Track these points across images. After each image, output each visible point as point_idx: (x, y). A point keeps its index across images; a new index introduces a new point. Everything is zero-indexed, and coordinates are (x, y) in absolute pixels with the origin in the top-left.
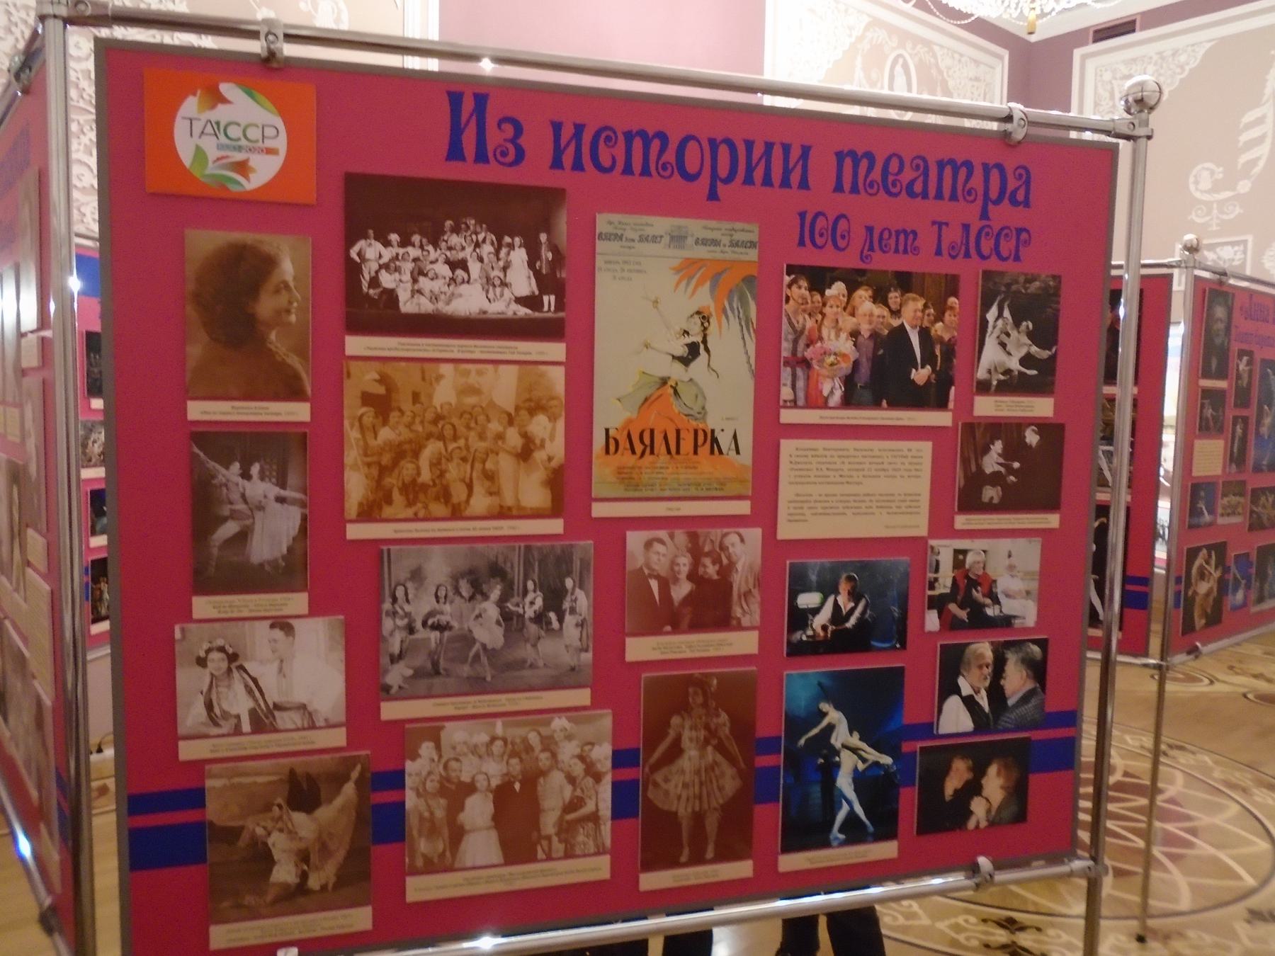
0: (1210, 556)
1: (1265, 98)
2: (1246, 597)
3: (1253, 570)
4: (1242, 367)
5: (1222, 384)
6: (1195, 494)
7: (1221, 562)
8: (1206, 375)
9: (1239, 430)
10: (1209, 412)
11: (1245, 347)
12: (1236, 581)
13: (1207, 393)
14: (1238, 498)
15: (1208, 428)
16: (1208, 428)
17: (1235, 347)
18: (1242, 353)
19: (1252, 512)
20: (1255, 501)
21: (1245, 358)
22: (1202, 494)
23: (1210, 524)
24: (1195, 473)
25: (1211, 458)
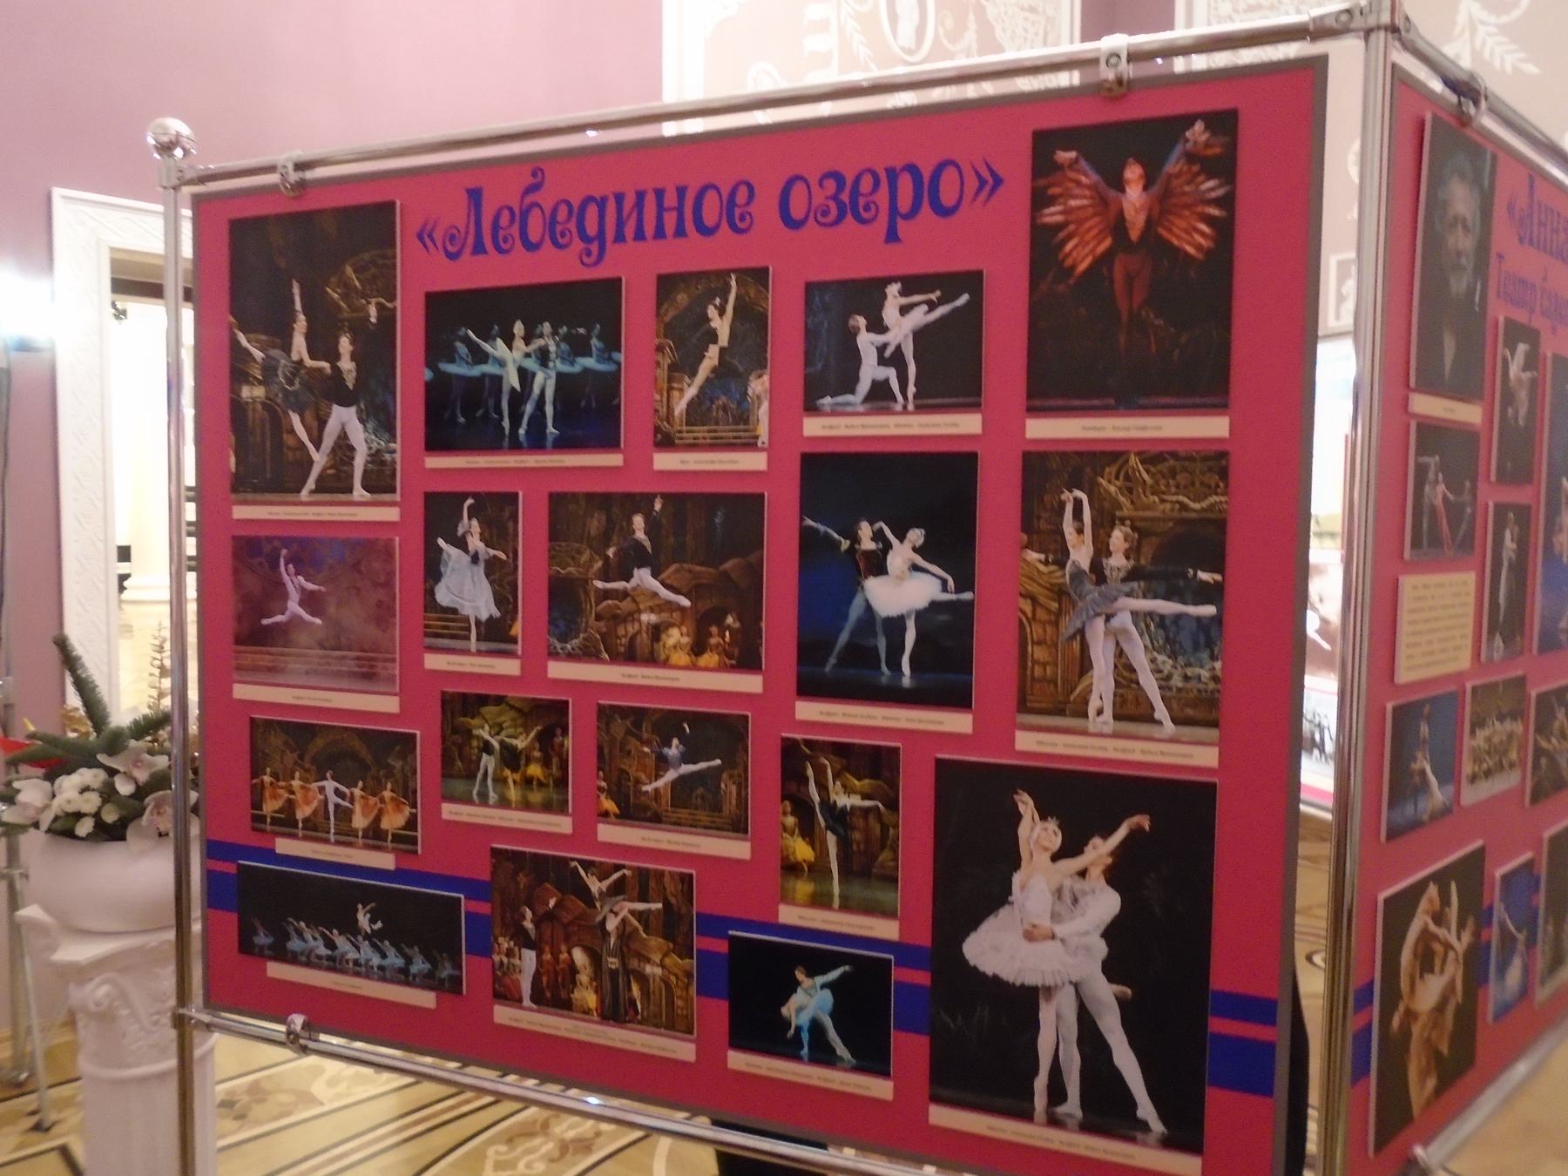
0: (1445, 899)
1: (1458, 29)
2: (1527, 970)
3: (1541, 899)
4: (1514, 369)
5: (1469, 414)
6: (1401, 731)
7: (1475, 911)
8: (1431, 386)
9: (1509, 544)
10: (1437, 493)
11: (1521, 316)
12: (1508, 941)
13: (1432, 433)
14: (1509, 725)
15: (1436, 541)
16: (1436, 541)
17: (1499, 312)
18: (1517, 332)
19: (1539, 752)
20: (1543, 728)
21: (1522, 348)
22: (1424, 729)
23: (1446, 811)
24: (1404, 676)
25: (1442, 621)
